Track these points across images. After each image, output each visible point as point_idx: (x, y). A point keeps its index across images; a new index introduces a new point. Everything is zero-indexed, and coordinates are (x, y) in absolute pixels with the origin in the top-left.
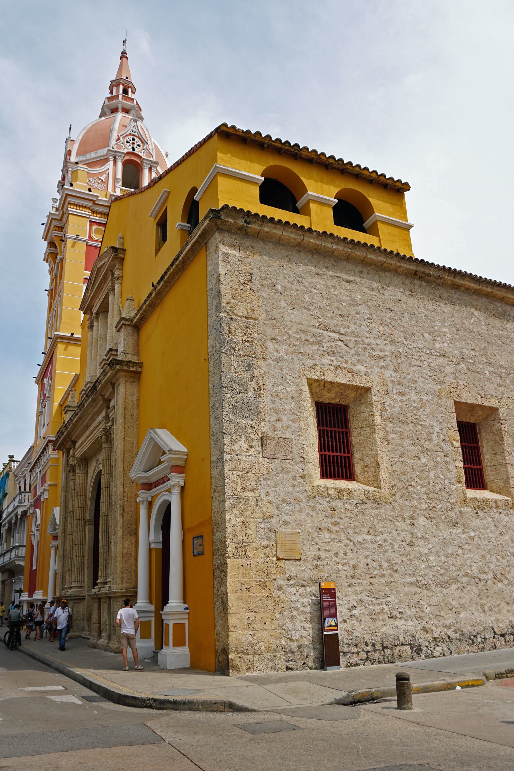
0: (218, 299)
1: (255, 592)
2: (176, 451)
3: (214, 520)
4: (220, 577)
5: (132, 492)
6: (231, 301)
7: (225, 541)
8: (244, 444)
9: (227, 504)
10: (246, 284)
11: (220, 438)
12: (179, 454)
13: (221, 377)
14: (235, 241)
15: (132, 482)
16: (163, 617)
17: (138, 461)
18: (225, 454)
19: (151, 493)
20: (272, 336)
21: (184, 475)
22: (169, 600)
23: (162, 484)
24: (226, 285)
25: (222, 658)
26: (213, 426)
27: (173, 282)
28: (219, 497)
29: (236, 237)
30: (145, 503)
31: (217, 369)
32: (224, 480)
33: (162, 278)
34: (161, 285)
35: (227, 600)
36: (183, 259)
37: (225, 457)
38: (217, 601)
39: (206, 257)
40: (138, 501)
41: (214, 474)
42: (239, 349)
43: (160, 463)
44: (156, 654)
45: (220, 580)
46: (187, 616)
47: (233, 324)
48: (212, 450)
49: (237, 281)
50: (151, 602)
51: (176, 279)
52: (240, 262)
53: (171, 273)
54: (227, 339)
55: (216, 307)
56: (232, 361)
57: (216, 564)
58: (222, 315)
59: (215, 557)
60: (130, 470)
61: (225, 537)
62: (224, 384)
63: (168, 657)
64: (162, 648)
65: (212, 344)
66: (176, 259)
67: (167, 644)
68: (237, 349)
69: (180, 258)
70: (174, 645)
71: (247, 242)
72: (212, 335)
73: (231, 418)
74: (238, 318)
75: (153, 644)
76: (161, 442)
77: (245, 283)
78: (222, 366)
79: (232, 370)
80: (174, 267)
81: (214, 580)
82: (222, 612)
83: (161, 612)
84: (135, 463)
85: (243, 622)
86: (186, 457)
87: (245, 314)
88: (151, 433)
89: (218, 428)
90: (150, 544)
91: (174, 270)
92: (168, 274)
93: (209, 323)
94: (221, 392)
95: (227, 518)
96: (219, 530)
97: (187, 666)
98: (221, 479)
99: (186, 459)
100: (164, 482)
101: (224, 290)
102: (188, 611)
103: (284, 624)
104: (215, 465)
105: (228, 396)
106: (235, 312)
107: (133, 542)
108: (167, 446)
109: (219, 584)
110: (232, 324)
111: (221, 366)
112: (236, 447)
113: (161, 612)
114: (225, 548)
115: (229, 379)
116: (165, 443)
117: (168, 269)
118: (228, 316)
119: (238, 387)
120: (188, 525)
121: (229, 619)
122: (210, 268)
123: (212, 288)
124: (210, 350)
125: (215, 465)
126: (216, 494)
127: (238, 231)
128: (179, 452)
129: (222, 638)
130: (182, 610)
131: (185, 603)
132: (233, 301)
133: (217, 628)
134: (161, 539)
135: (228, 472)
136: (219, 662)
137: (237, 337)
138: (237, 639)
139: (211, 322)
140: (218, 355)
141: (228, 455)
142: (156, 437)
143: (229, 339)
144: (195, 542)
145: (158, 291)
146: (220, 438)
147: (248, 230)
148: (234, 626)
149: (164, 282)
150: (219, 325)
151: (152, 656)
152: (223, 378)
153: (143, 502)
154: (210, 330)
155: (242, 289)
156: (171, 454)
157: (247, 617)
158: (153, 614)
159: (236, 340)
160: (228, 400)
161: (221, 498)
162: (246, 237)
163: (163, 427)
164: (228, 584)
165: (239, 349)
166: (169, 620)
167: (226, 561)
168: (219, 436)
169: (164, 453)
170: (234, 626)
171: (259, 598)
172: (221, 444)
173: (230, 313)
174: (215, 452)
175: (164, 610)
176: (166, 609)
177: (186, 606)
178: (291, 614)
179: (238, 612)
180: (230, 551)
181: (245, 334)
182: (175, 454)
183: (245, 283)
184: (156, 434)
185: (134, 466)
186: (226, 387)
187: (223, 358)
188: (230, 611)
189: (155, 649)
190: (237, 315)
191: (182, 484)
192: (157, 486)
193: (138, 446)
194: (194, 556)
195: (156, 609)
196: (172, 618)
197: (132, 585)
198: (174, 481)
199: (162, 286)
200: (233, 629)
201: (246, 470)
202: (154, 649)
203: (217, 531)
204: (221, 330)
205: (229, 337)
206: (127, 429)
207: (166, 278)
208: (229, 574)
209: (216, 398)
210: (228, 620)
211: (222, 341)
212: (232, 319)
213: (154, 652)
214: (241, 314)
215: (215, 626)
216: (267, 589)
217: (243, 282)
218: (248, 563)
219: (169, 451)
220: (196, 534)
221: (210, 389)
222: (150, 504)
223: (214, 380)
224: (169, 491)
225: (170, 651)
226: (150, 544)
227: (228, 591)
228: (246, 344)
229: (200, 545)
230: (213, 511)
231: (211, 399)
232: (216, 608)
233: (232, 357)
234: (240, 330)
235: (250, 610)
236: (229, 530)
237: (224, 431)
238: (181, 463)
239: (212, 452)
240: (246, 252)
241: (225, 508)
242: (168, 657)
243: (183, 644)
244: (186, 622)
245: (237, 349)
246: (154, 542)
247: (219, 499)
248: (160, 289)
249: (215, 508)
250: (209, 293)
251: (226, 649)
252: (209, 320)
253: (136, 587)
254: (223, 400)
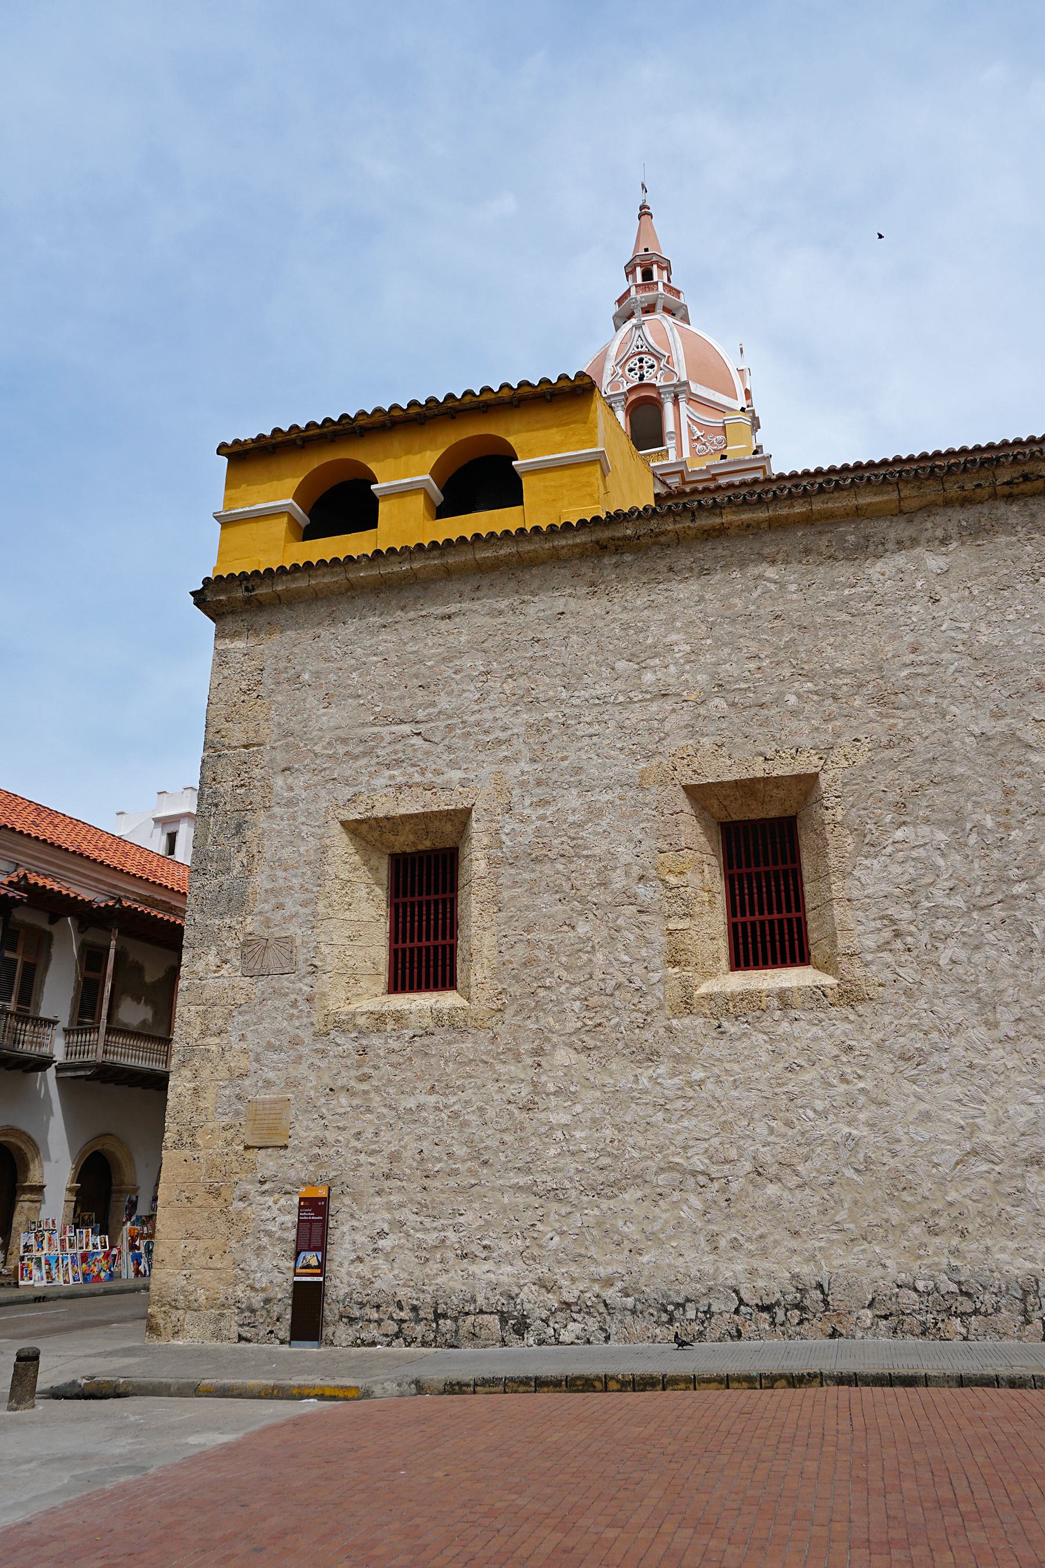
1: (200, 1203)
8: (212, 959)
20: (284, 766)
42: (225, 803)
71: (262, 619)
79: (209, 840)
87: (244, 741)
103: (244, 1261)
157: (183, 1246)
165: (225, 803)
171: (206, 1214)
173: (219, 746)
178: (258, 1243)
183: (249, 690)
201: (211, 1001)
216: (221, 1200)
218: (195, 1156)
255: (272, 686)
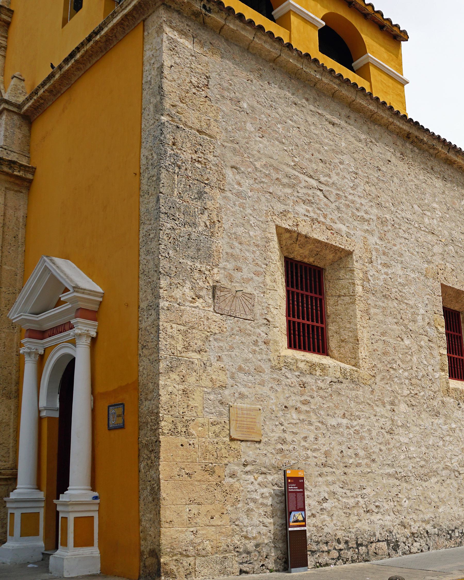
0: (158, 98)
1: (199, 478)
2: (85, 290)
3: (141, 384)
4: (149, 458)
5: (12, 340)
6: (177, 103)
7: (158, 413)
8: (189, 294)
9: (162, 365)
10: (201, 88)
11: (155, 279)
12: (89, 294)
13: (158, 200)
14: (188, 28)
15: (12, 326)
16: (59, 509)
17: (23, 298)
18: (160, 301)
19: (42, 344)
21: (96, 323)
22: (68, 486)
23: (61, 332)
24: (171, 81)
25: (150, 561)
26: (143, 262)
27: (89, 65)
28: (150, 355)
29: (189, 23)
30: (33, 355)
31: (153, 189)
32: (159, 333)
33: (72, 55)
34: (70, 64)
35: (159, 489)
36: (106, 34)
37: (161, 305)
38: (144, 489)
39: (144, 38)
40: (21, 352)
41: (143, 325)
42: (186, 169)
43: (59, 303)
44: (46, 557)
45: (149, 462)
46: (96, 508)
47: (179, 135)
48: (141, 293)
49: (188, 80)
50: (39, 488)
51: (94, 61)
52: (194, 58)
53: (87, 51)
54: (170, 152)
55: (156, 106)
56: (176, 183)
57: (144, 442)
58: (164, 119)
59: (142, 433)
60: (9, 310)
61: (158, 407)
62: (163, 210)
63: (65, 562)
64: (57, 548)
65: (146, 154)
66: (96, 33)
67: (65, 544)
68: (184, 168)
69: (103, 33)
70: (76, 545)
71: (205, 35)
72: (148, 143)
73: (172, 255)
74: (187, 129)
75: (41, 544)
76: (62, 275)
77: (198, 87)
78: (161, 185)
79: (176, 193)
80: (91, 43)
81: (139, 462)
82: (151, 503)
83: (55, 501)
84: (18, 300)
85: (181, 517)
86: (101, 299)
87: (198, 127)
88: (45, 261)
89: (151, 265)
90: (39, 412)
91: (92, 47)
92: (82, 52)
93: (143, 126)
94: (157, 218)
95: (161, 382)
96: (149, 397)
97: (95, 573)
98: (153, 332)
99: (101, 302)
100: (65, 330)
101: (169, 87)
102: (98, 501)
104: (145, 313)
105: (169, 226)
106: (183, 119)
107: (13, 408)
108: (72, 281)
109: (147, 468)
110: (178, 135)
111: (159, 185)
112: (177, 293)
113: (55, 501)
114: (157, 421)
115: (170, 204)
116: (68, 277)
117: (82, 44)
118: (172, 123)
119: (183, 217)
120: (100, 389)
121: (162, 512)
122: (148, 54)
123: (150, 81)
124: (144, 161)
125: (145, 313)
126: (146, 352)
127: (193, 17)
128: (91, 291)
129: (151, 536)
130: (89, 499)
131: (93, 489)
132: (181, 105)
133: (143, 523)
134: (58, 406)
135: (165, 324)
136: (145, 567)
137: (185, 153)
138: (174, 537)
139: (147, 125)
140: (155, 170)
141: (165, 302)
142: (54, 267)
143: (172, 152)
144: (112, 411)
145: (65, 72)
146: (155, 279)
147: (207, 20)
148: (168, 521)
149: (76, 61)
150: (159, 132)
151: (40, 559)
152: (162, 201)
153: (29, 354)
154: (144, 136)
155: (194, 94)
156: (77, 292)
157: (188, 510)
158: (43, 504)
159: (182, 155)
160: (168, 231)
161: (153, 357)
162: (203, 29)
163: (66, 257)
164: (161, 468)
165: (186, 169)
166: (69, 512)
167: (159, 438)
168: (153, 276)
169: (66, 290)
170: (168, 521)
171: (204, 486)
172: (155, 288)
173: (177, 120)
174: (146, 297)
175: (61, 499)
176: (63, 498)
177: (96, 494)
179: (174, 503)
180: (165, 425)
181: (196, 152)
182: (83, 293)
183: (198, 87)
184: (54, 263)
185: (16, 305)
186: (166, 213)
187: (163, 175)
188: (162, 502)
189: (46, 550)
190: (185, 125)
191: (94, 334)
192: (54, 334)
193: (24, 279)
194: (110, 429)
195: (47, 498)
196: (72, 510)
197: (9, 464)
198: (81, 329)
199: (72, 67)
200: (167, 525)
201: (190, 324)
202: (43, 550)
203: (146, 399)
204: (162, 138)
205: (172, 150)
206: (6, 253)
207: (78, 56)
208: (162, 455)
209: (150, 226)
210: (159, 513)
211: (163, 152)
212: (178, 127)
213: (43, 554)
214: (191, 125)
215: (140, 521)
216: (215, 476)
217: (196, 84)
218: (191, 442)
219: (74, 287)
220: (113, 402)
221: (141, 214)
222: (41, 360)
223: (148, 203)
224: (73, 343)
225: (69, 554)
226: (39, 412)
227: (161, 476)
228: (196, 164)
229: (119, 416)
230: (141, 373)
231: (141, 227)
232: (142, 498)
233: (176, 177)
234: (189, 145)
235: (191, 501)
236: (164, 398)
237: (161, 270)
238: (94, 307)
239: (141, 296)
240: (202, 47)
241: (158, 370)
242: (65, 561)
243: (90, 543)
244: (96, 515)
245: (184, 168)
246: (46, 409)
247: (151, 358)
248: (68, 70)
249: (144, 369)
250: (145, 86)
251: (157, 551)
252: (143, 123)
253: (15, 467)
254: (161, 230)
255: (218, 96)
